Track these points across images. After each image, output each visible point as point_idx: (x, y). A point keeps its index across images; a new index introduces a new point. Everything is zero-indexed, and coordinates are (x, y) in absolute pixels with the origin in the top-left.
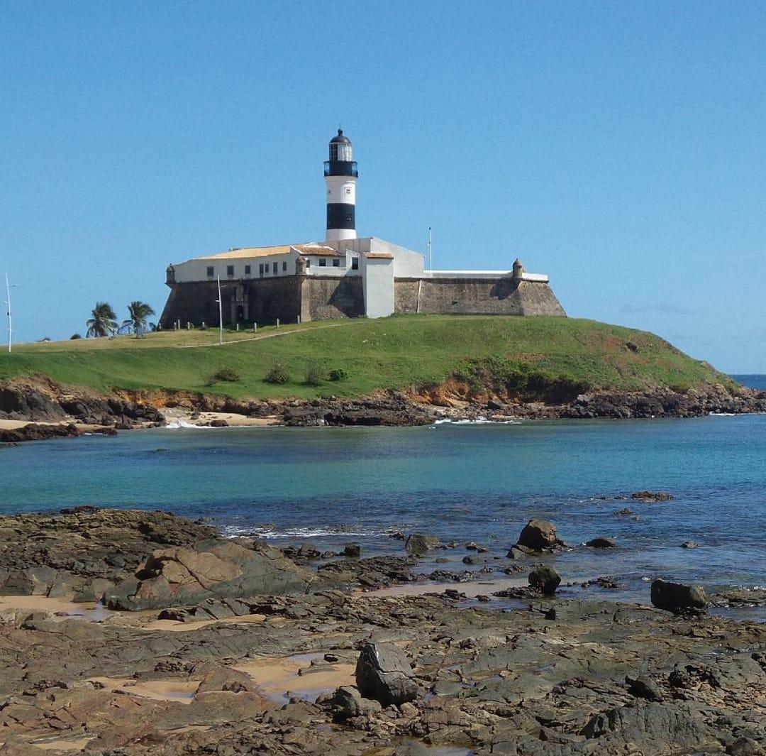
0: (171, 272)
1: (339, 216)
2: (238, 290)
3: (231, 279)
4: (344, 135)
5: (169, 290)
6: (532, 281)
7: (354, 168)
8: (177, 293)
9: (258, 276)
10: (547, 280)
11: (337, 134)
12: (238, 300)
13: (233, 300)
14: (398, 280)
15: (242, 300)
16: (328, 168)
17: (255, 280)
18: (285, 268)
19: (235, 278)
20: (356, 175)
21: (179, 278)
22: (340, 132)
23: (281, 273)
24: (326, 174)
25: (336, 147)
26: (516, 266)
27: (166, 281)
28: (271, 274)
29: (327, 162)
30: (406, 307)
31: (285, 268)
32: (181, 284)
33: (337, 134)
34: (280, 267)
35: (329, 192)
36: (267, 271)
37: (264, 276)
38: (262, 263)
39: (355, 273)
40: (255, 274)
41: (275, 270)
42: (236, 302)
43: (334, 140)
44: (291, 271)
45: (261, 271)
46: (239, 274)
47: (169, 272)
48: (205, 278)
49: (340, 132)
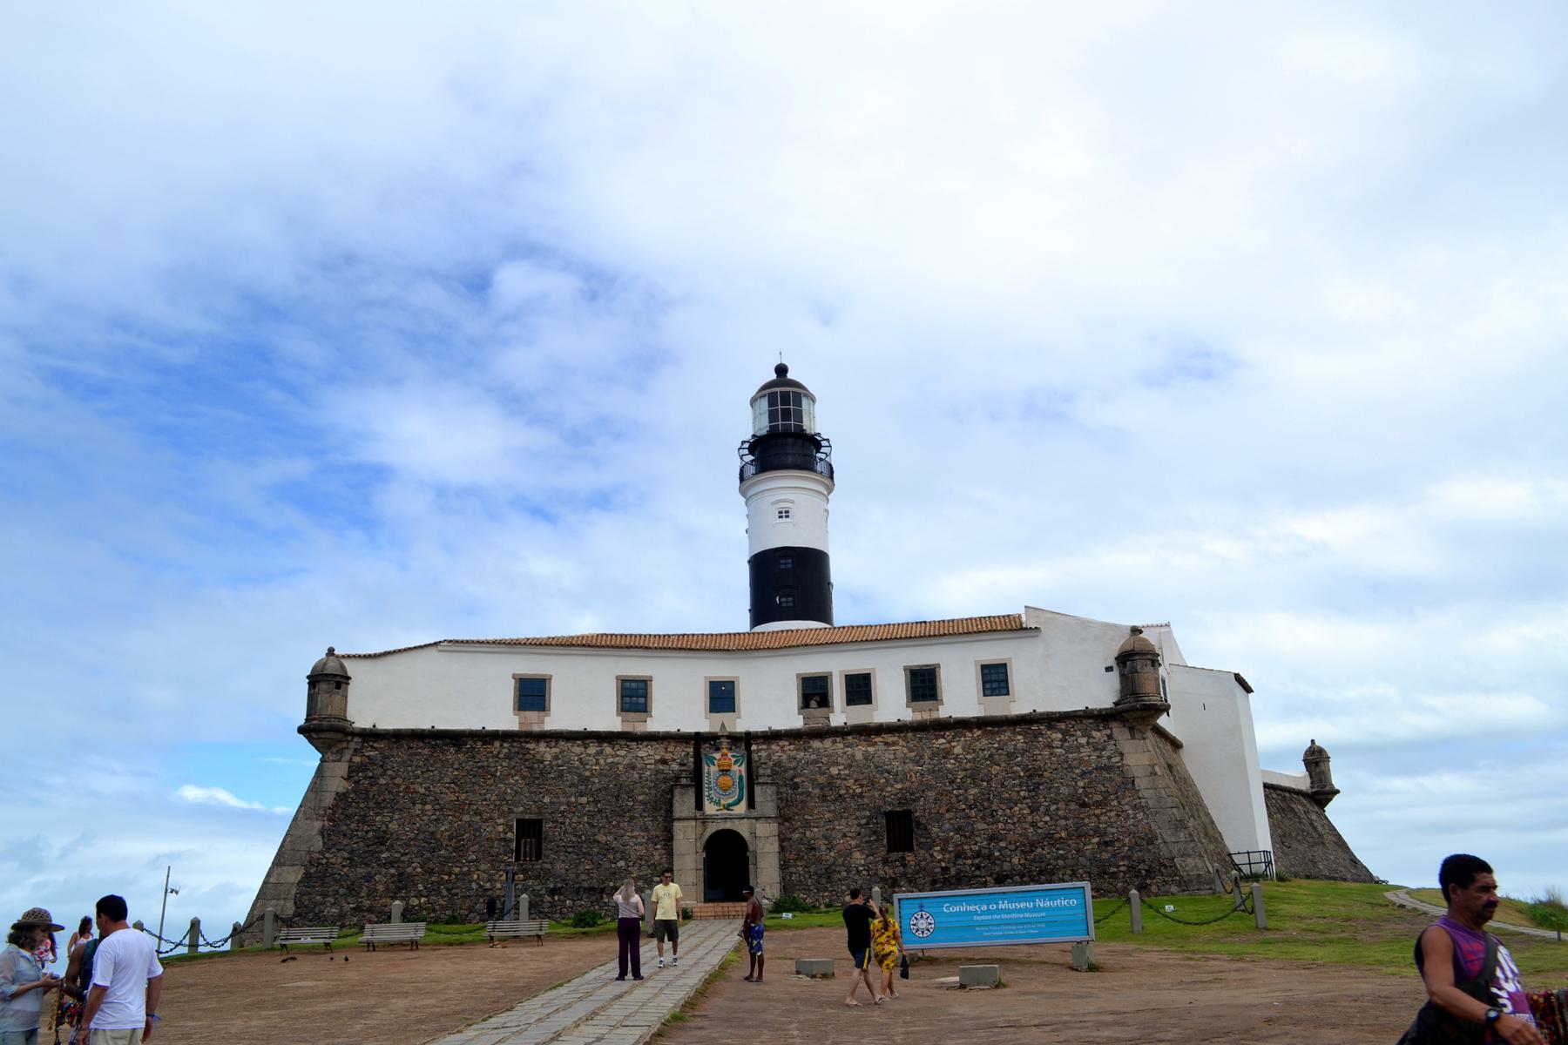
0: (328, 680)
1: (789, 583)
2: (710, 771)
3: (640, 728)
4: (790, 376)
8: (342, 768)
9: (789, 717)
11: (774, 376)
12: (710, 808)
13: (683, 804)
15: (741, 808)
17: (772, 737)
19: (655, 724)
21: (369, 707)
22: (781, 370)
23: (961, 697)
26: (1316, 759)
27: (301, 721)
28: (891, 703)
32: (372, 736)
37: (840, 714)
42: (705, 820)
47: (315, 679)
49: (781, 370)
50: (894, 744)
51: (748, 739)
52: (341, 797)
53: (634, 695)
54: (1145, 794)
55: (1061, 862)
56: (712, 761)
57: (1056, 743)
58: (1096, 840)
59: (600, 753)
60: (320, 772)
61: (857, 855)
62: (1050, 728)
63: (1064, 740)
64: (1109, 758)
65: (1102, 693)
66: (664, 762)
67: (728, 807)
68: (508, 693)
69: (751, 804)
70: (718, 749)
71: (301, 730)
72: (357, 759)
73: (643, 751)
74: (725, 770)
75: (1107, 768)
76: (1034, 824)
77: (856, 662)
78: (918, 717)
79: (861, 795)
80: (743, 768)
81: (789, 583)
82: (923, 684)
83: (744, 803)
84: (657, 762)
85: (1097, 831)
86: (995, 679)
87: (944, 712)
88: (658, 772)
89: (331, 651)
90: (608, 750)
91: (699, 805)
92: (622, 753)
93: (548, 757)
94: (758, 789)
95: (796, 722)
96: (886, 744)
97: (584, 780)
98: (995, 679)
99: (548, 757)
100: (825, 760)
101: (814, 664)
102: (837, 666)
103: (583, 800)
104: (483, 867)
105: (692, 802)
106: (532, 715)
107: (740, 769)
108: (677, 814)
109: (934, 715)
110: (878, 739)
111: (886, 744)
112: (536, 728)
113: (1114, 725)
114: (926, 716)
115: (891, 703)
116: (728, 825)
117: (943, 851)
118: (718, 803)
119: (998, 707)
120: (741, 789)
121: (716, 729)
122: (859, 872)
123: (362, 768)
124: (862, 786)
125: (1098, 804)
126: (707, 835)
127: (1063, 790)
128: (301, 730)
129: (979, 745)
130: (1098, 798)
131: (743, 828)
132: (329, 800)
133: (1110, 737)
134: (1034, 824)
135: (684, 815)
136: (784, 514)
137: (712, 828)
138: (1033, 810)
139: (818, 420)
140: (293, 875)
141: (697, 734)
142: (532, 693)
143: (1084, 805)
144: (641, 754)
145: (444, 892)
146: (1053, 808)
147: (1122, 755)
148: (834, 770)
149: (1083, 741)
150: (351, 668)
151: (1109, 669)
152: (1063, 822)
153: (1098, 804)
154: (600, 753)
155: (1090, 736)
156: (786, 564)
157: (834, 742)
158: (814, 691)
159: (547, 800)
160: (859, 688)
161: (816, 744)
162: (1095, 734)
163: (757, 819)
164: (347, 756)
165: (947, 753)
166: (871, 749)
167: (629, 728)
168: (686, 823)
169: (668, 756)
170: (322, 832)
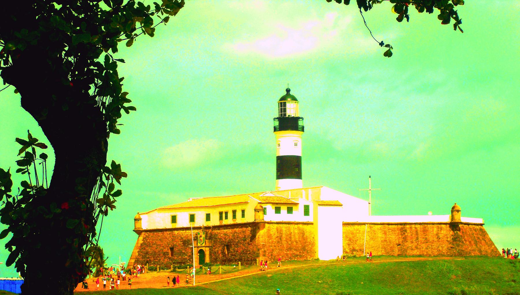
6: (468, 224)
7: (300, 123)
8: (141, 238)
9: (217, 223)
10: (482, 223)
11: (285, 93)
12: (199, 245)
14: (345, 224)
16: (277, 123)
18: (243, 216)
20: (303, 129)
22: (288, 91)
24: (275, 129)
25: (285, 103)
26: (454, 210)
29: (277, 118)
30: (354, 250)
31: (243, 216)
32: (146, 231)
33: (285, 93)
34: (239, 214)
35: (279, 145)
36: (226, 218)
37: (225, 222)
38: (221, 211)
39: (306, 219)
40: (215, 221)
41: (234, 216)
42: (198, 247)
43: (283, 98)
44: (250, 218)
45: (221, 218)
46: (200, 221)
48: (169, 225)
49: (288, 91)
52: (141, 244)
53: (192, 218)
73: (193, 232)
97: (182, 238)
107: (203, 236)
131: (203, 249)
132: (139, 245)
137: (200, 249)
140: (133, 261)
142: (174, 219)
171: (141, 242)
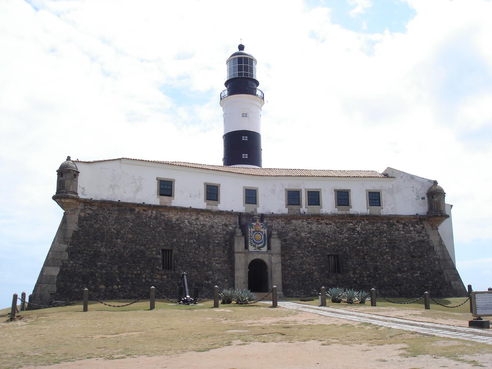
0: (67, 174)
1: (242, 147)
3: (214, 208)
4: (245, 51)
5: (56, 214)
8: (75, 218)
11: (237, 50)
12: (251, 248)
13: (239, 246)
15: (265, 249)
22: (241, 47)
23: (359, 205)
27: (54, 192)
32: (89, 203)
37: (304, 208)
49: (241, 47)
50: (330, 224)
51: (262, 217)
52: (76, 233)
53: (212, 193)
54: (439, 253)
55: (405, 281)
56: (252, 226)
57: (401, 229)
58: (419, 272)
59: (197, 219)
60: (64, 221)
61: (316, 273)
62: (398, 222)
63: (404, 228)
64: (423, 237)
65: (421, 209)
66: (226, 225)
67: (259, 248)
68: (154, 188)
69: (269, 248)
70: (255, 221)
71: (54, 198)
72: (82, 214)
74: (257, 231)
75: (423, 241)
76: (393, 264)
77: (313, 186)
78: (340, 212)
79: (315, 246)
80: (266, 230)
81: (242, 147)
82: (343, 198)
83: (266, 247)
84: (223, 225)
85: (419, 268)
86: (374, 198)
87: (352, 211)
88: (224, 230)
89: (69, 158)
90: (201, 218)
91: (246, 247)
92: (207, 220)
93: (174, 220)
94: (272, 240)
95: (285, 210)
96: (326, 224)
98: (374, 198)
99: (174, 220)
100: (298, 229)
101: (293, 185)
102: (305, 186)
103: (192, 241)
104: (147, 271)
105: (243, 246)
106: (166, 199)
108: (236, 250)
109: (348, 212)
110: (323, 222)
111: (326, 224)
112: (168, 205)
113: (424, 222)
114: (344, 212)
115: (328, 205)
116: (259, 257)
117: (354, 273)
118: (255, 246)
119: (375, 210)
120: (265, 241)
121: (249, 211)
122: (317, 281)
123: (85, 219)
124: (316, 242)
125: (420, 257)
126: (249, 262)
127: (405, 250)
128: (54, 198)
129: (367, 227)
130: (419, 254)
131: (266, 258)
132: (70, 235)
133: (423, 228)
134: (393, 264)
135: (240, 250)
136: (245, 115)
138: (392, 258)
139: (259, 74)
140: (55, 271)
141: (240, 213)
142: (166, 188)
143: (413, 257)
144: (216, 221)
145: (130, 283)
146: (400, 257)
147: (428, 236)
148: (303, 234)
149: (412, 229)
150: (80, 168)
151: (423, 198)
152: (405, 264)
153: (420, 257)
154: (197, 219)
155: (415, 227)
156: (245, 138)
157: (303, 221)
158: (293, 197)
159: (175, 240)
160: (314, 197)
161: (294, 222)
162: (417, 226)
163: (272, 255)
164: (78, 212)
165: (354, 230)
166: (320, 226)
167: (210, 208)
168: (240, 255)
169: (227, 223)
170: (67, 250)
171: (73, 227)
